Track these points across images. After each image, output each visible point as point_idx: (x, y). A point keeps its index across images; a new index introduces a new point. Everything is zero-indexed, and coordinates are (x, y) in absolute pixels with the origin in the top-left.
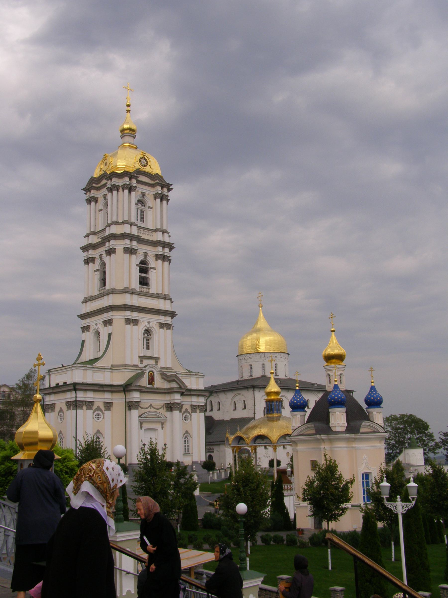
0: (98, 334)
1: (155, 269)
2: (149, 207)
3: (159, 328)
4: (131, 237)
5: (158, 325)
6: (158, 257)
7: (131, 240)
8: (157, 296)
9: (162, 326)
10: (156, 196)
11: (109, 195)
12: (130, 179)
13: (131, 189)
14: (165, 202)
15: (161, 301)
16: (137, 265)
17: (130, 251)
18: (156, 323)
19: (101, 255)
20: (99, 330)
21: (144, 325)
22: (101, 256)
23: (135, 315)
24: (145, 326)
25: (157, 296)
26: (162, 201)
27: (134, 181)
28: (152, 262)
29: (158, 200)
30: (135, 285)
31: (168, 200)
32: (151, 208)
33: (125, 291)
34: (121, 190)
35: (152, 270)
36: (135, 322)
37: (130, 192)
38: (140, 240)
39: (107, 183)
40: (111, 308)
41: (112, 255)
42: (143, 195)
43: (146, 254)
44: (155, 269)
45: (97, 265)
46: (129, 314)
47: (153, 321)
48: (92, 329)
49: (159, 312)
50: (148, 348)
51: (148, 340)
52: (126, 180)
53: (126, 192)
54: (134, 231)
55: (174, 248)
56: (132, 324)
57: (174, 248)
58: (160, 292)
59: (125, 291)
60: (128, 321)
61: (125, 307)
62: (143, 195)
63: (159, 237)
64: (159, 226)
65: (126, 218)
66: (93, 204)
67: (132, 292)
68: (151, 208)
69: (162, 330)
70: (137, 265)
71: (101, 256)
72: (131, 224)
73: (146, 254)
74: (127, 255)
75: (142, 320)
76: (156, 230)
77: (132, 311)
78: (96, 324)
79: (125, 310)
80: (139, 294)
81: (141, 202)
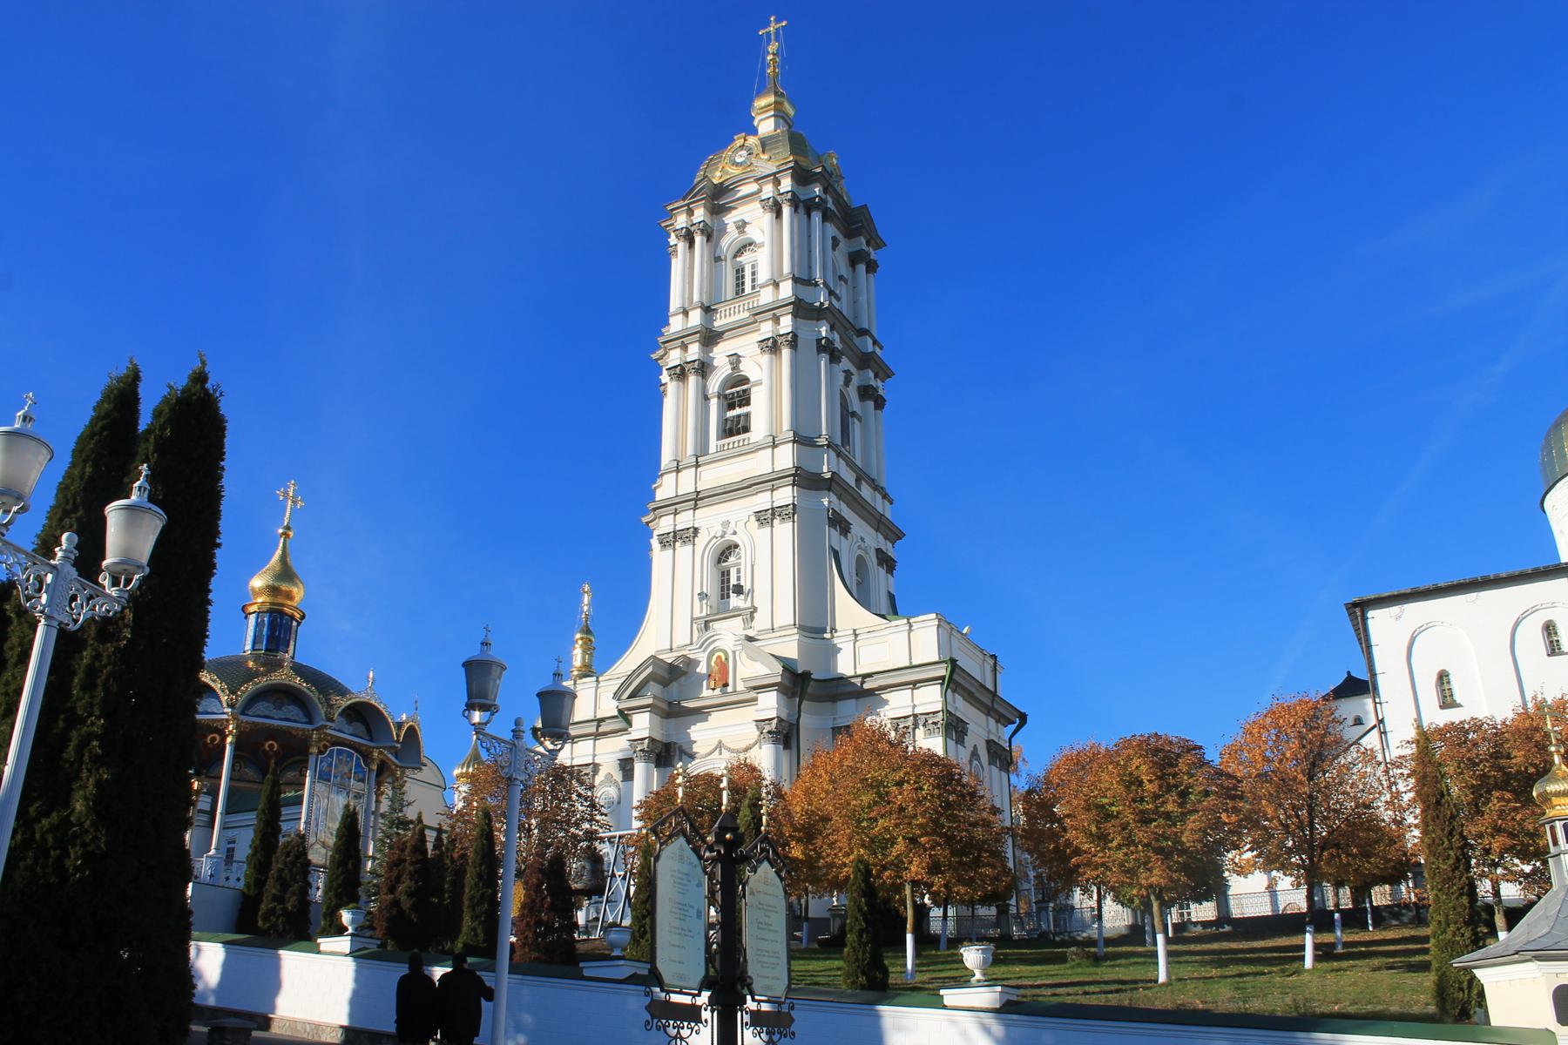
2: (841, 278)
11: (767, 218)
15: (879, 497)
20: (735, 539)
22: (735, 360)
29: (862, 268)
34: (801, 210)
39: (760, 191)
45: (714, 384)
48: (701, 540)
49: (880, 521)
53: (817, 217)
61: (832, 484)
71: (735, 360)
75: (854, 529)
78: (726, 524)
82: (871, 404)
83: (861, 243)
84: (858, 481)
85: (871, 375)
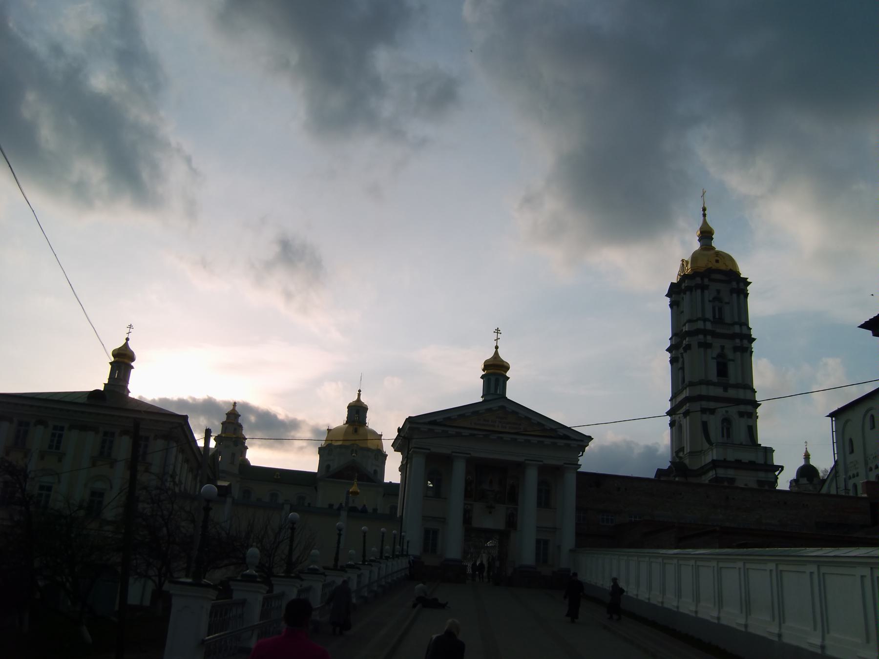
0: (680, 426)
4: (705, 332)
6: (736, 349)
7: (705, 336)
8: (737, 386)
9: (741, 414)
10: (732, 291)
12: (702, 279)
13: (703, 288)
14: (742, 296)
16: (713, 358)
17: (706, 346)
19: (682, 354)
23: (712, 405)
25: (737, 386)
26: (738, 296)
27: (706, 281)
28: (730, 354)
29: (735, 296)
30: (713, 376)
31: (746, 295)
32: (728, 303)
33: (701, 383)
36: (712, 411)
37: (703, 292)
38: (714, 334)
40: (687, 400)
41: (688, 351)
42: (718, 291)
43: (723, 348)
44: (733, 360)
47: (733, 411)
50: (728, 436)
51: (728, 429)
52: (698, 280)
53: (699, 291)
54: (709, 326)
55: (754, 339)
57: (754, 339)
59: (701, 383)
60: (704, 411)
61: (700, 398)
62: (718, 291)
63: (737, 329)
64: (737, 320)
65: (700, 315)
66: (675, 307)
67: (708, 383)
68: (728, 303)
70: (713, 358)
71: (682, 354)
72: (705, 320)
73: (723, 348)
74: (702, 350)
76: (735, 323)
80: (714, 384)
81: (717, 299)
83: (734, 285)
84: (725, 390)
85: (738, 341)
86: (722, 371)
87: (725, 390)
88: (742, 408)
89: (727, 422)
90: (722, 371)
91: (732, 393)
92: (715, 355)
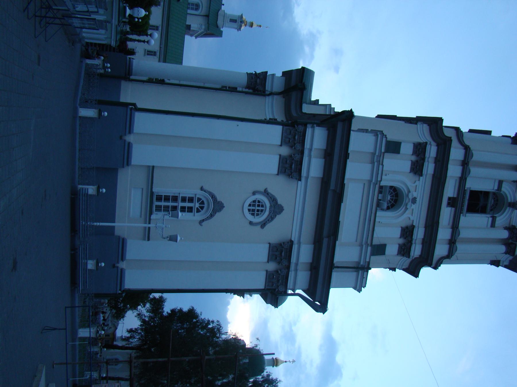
1: (493, 225)
3: (404, 225)
5: (409, 223)
8: (455, 227)
9: (407, 232)
16: (500, 183)
18: (411, 219)
21: (412, 189)
23: (429, 168)
24: (409, 192)
25: (455, 227)
35: (490, 219)
36: (417, 169)
44: (493, 225)
46: (432, 151)
56: (414, 158)
58: (461, 236)
60: (420, 149)
69: (397, 232)
70: (500, 183)
77: (437, 161)
79: (438, 145)
82: (505, 234)
84: (452, 202)
86: (479, 202)
87: (452, 202)
88: (419, 234)
89: (394, 198)
90: (479, 202)
91: (446, 214)
92: (506, 189)
